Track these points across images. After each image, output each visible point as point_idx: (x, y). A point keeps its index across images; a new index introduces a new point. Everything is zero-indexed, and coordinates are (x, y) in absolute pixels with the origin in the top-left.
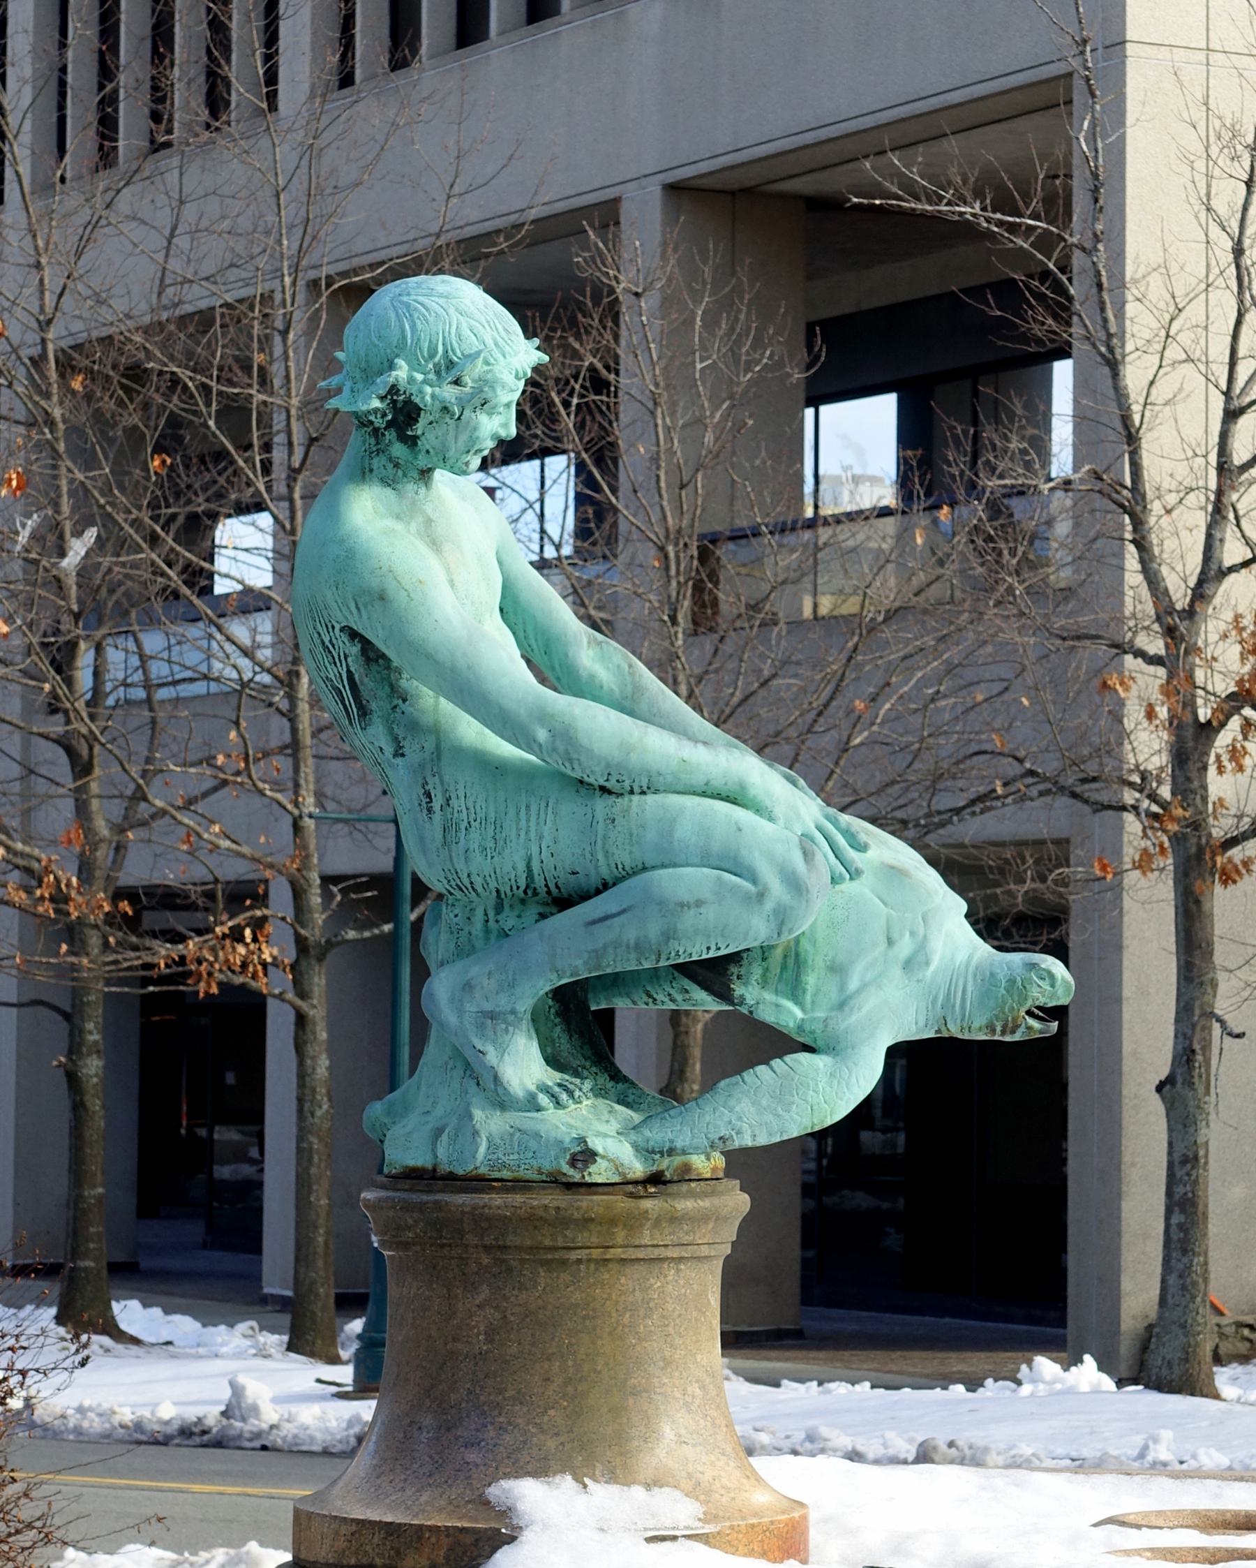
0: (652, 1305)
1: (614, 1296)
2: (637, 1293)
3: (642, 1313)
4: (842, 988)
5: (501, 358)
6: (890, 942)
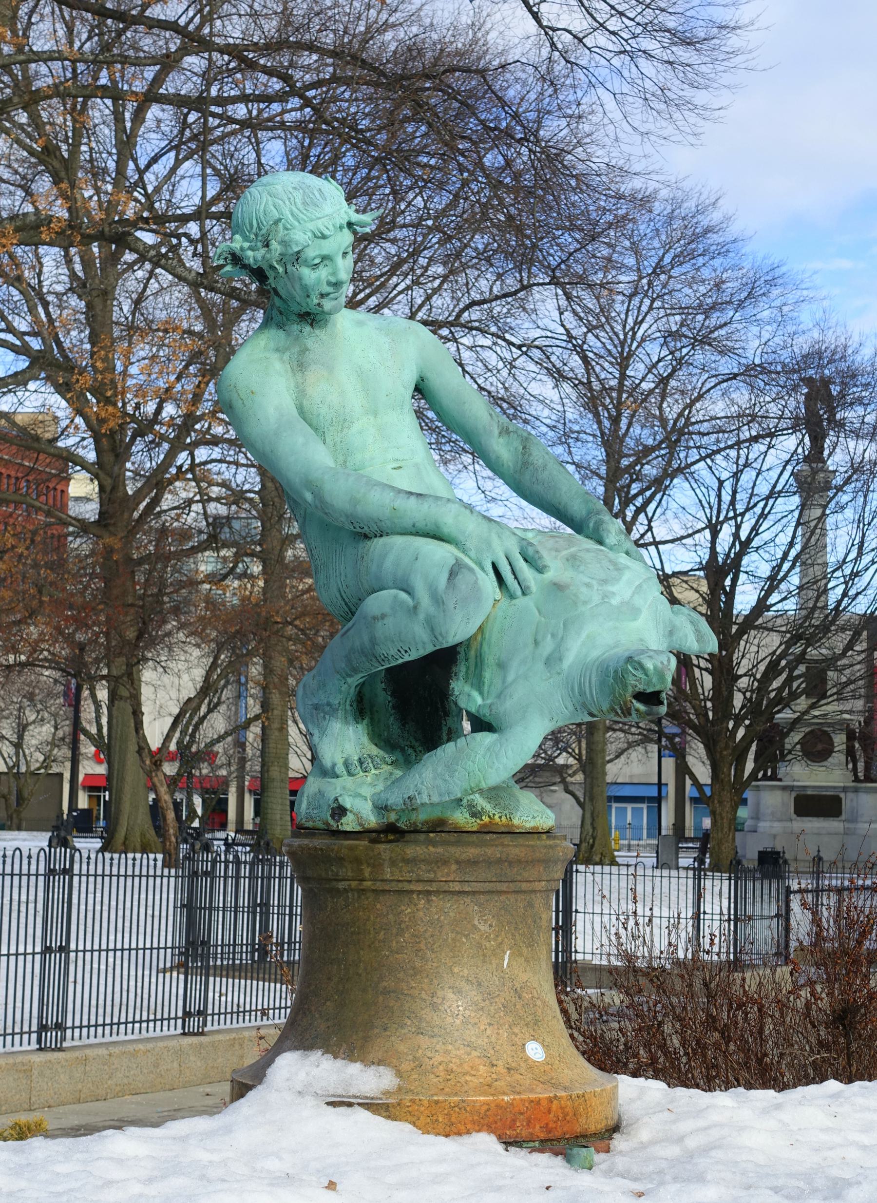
0: (403, 926)
1: (372, 918)
2: (391, 917)
3: (394, 931)
4: (504, 681)
5: (297, 224)
6: (536, 643)
